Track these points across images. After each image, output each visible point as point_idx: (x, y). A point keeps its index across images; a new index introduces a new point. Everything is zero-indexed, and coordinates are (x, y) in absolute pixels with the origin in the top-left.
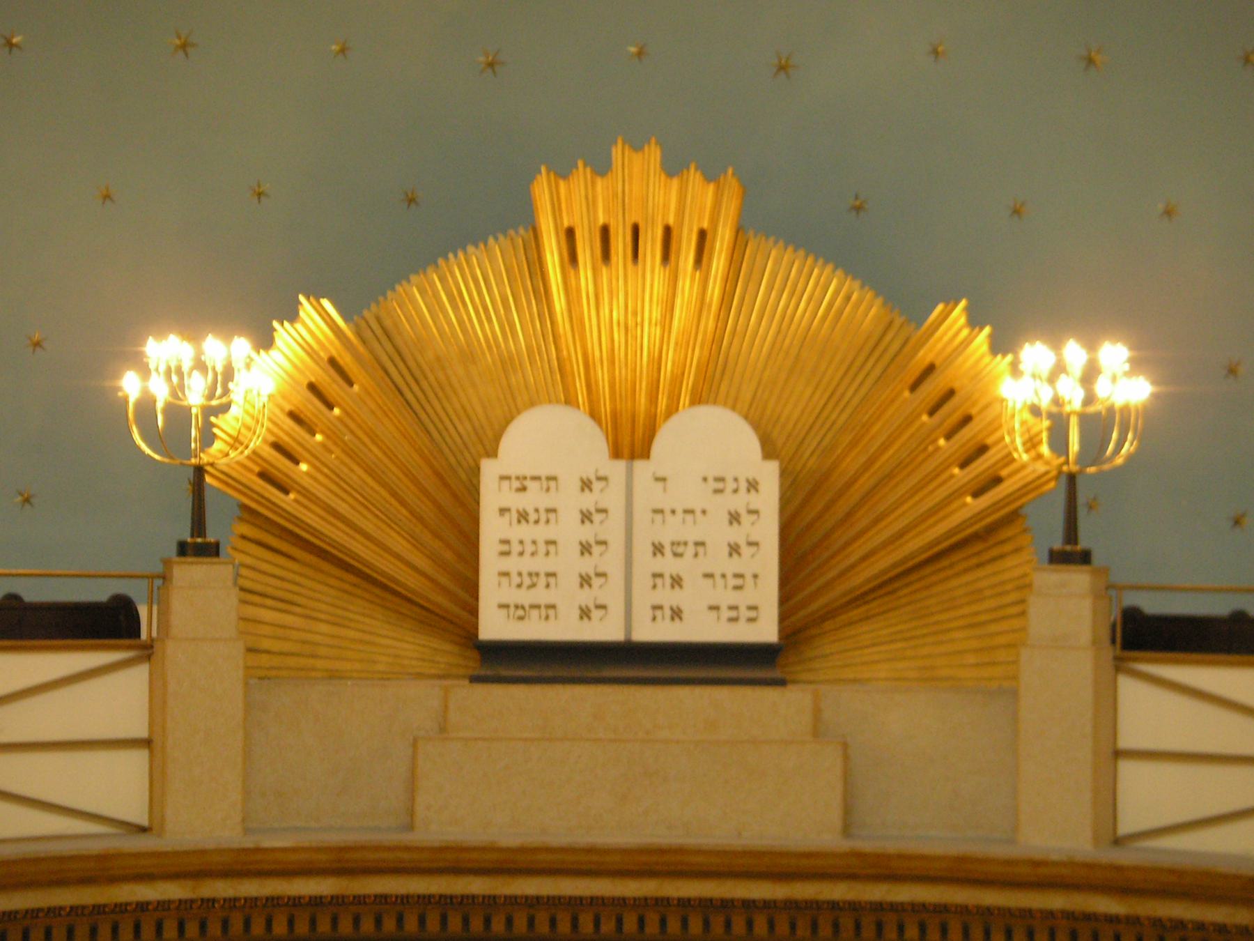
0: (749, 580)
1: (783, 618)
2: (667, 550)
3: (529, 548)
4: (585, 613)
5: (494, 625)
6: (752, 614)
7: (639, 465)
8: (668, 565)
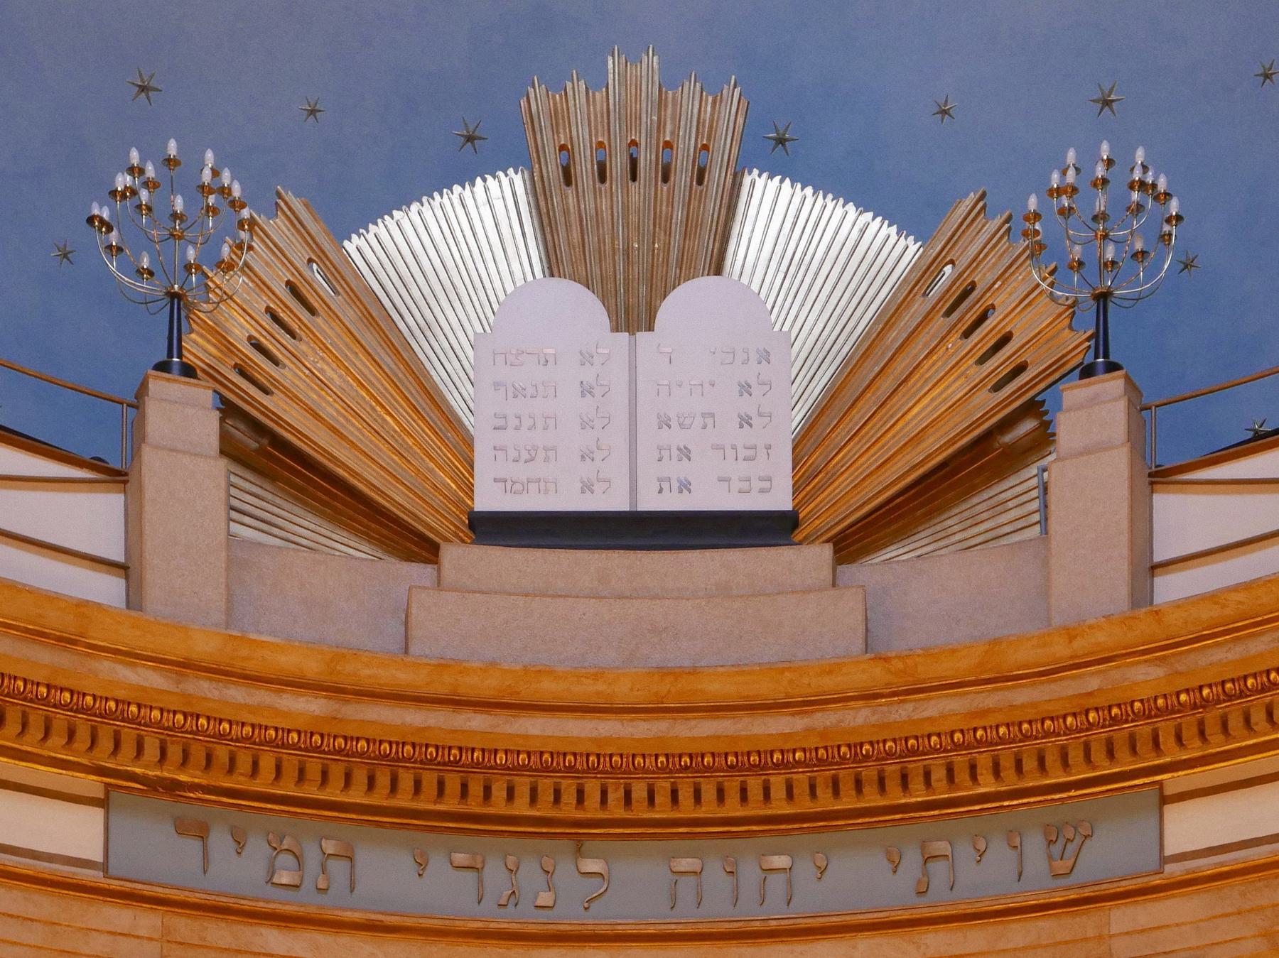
0: (762, 452)
1: (796, 489)
2: (674, 423)
3: (527, 422)
4: (587, 487)
5: (488, 499)
6: (766, 485)
7: (642, 336)
8: (676, 437)
